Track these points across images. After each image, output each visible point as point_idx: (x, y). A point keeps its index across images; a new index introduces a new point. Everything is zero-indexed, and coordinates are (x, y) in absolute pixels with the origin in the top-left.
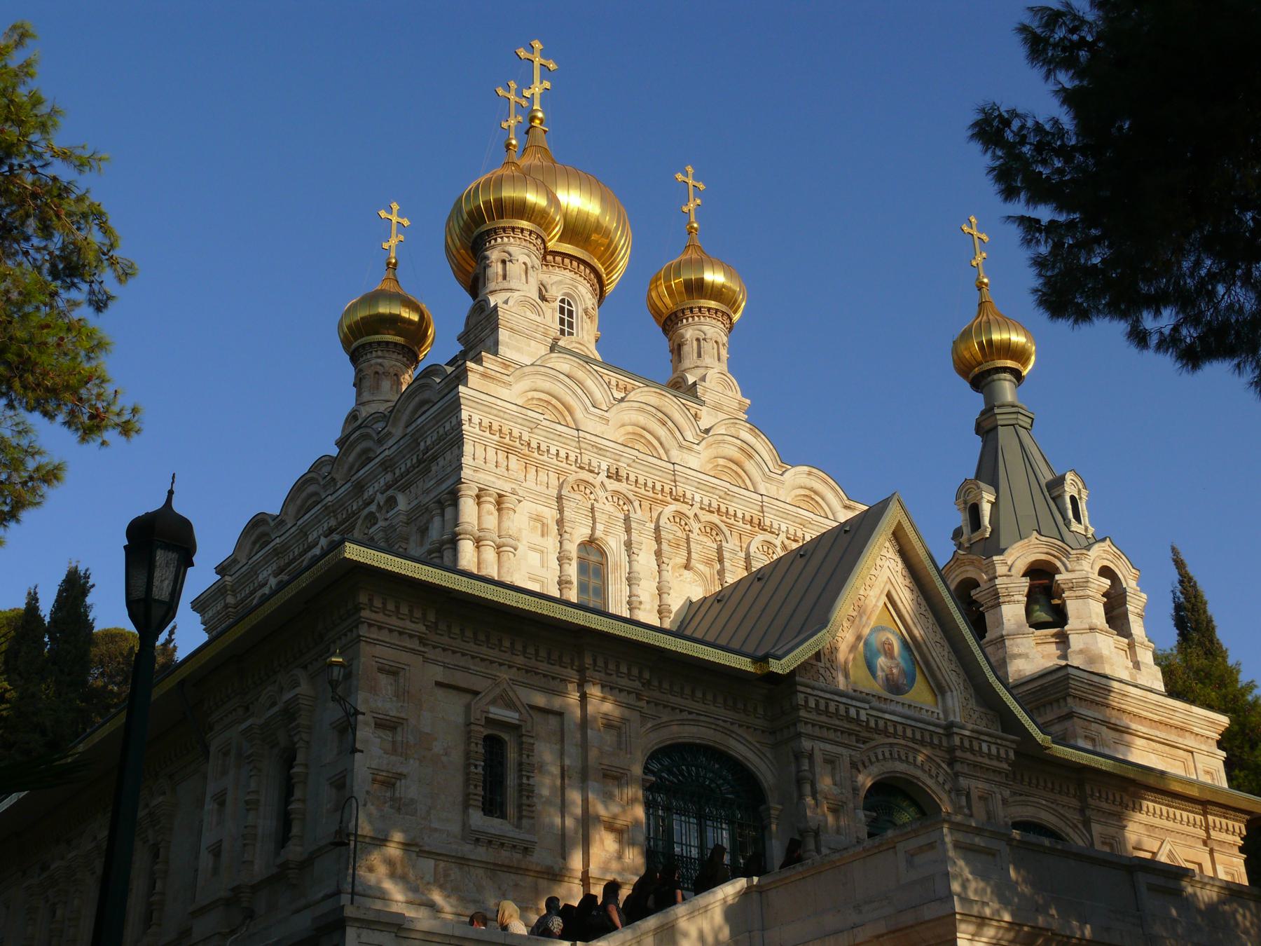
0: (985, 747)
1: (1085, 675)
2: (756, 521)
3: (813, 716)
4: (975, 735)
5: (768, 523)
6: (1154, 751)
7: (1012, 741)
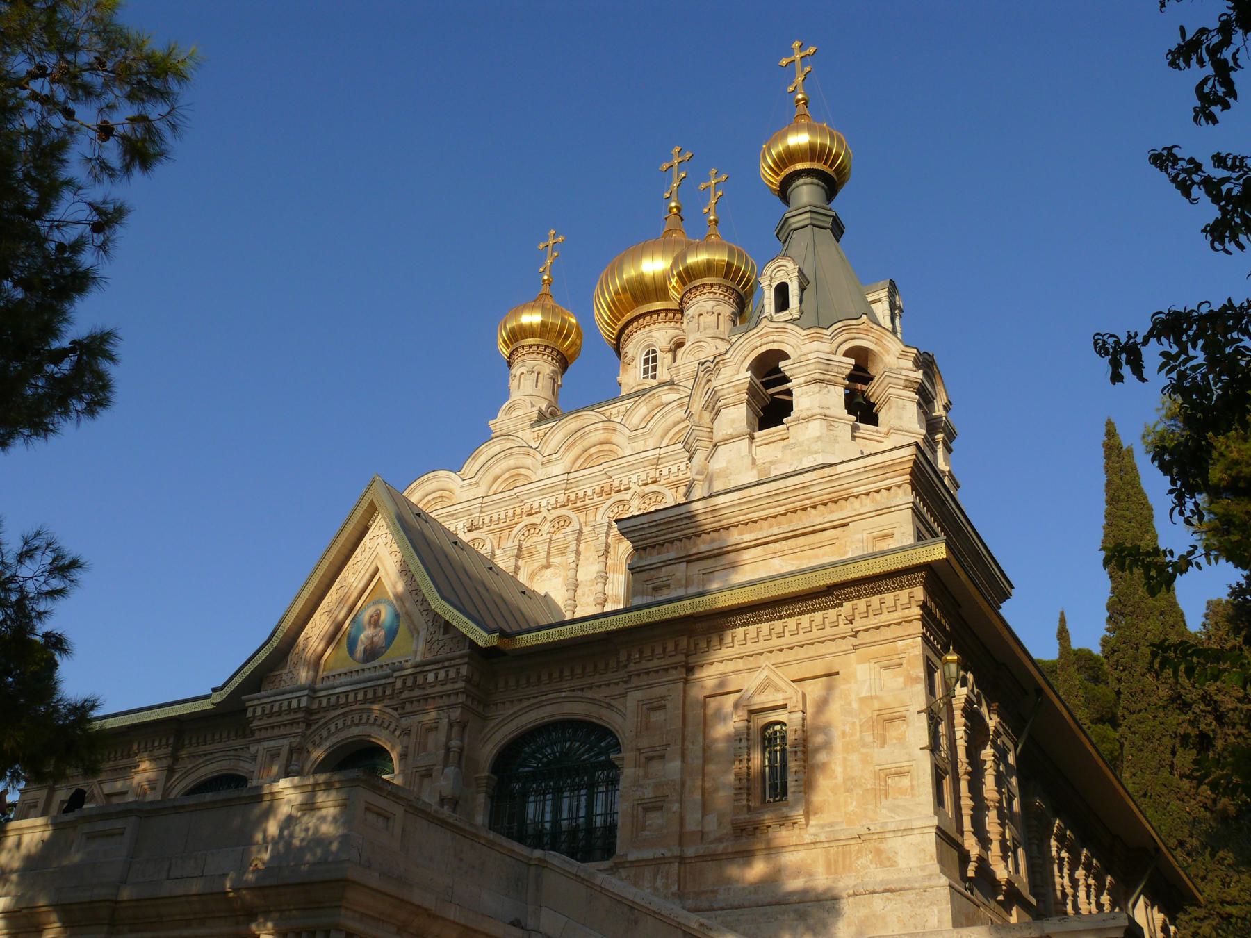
0: (431, 677)
1: (644, 519)
2: (607, 489)
3: (265, 721)
4: (418, 669)
5: (616, 483)
6: (776, 554)
7: (462, 657)
